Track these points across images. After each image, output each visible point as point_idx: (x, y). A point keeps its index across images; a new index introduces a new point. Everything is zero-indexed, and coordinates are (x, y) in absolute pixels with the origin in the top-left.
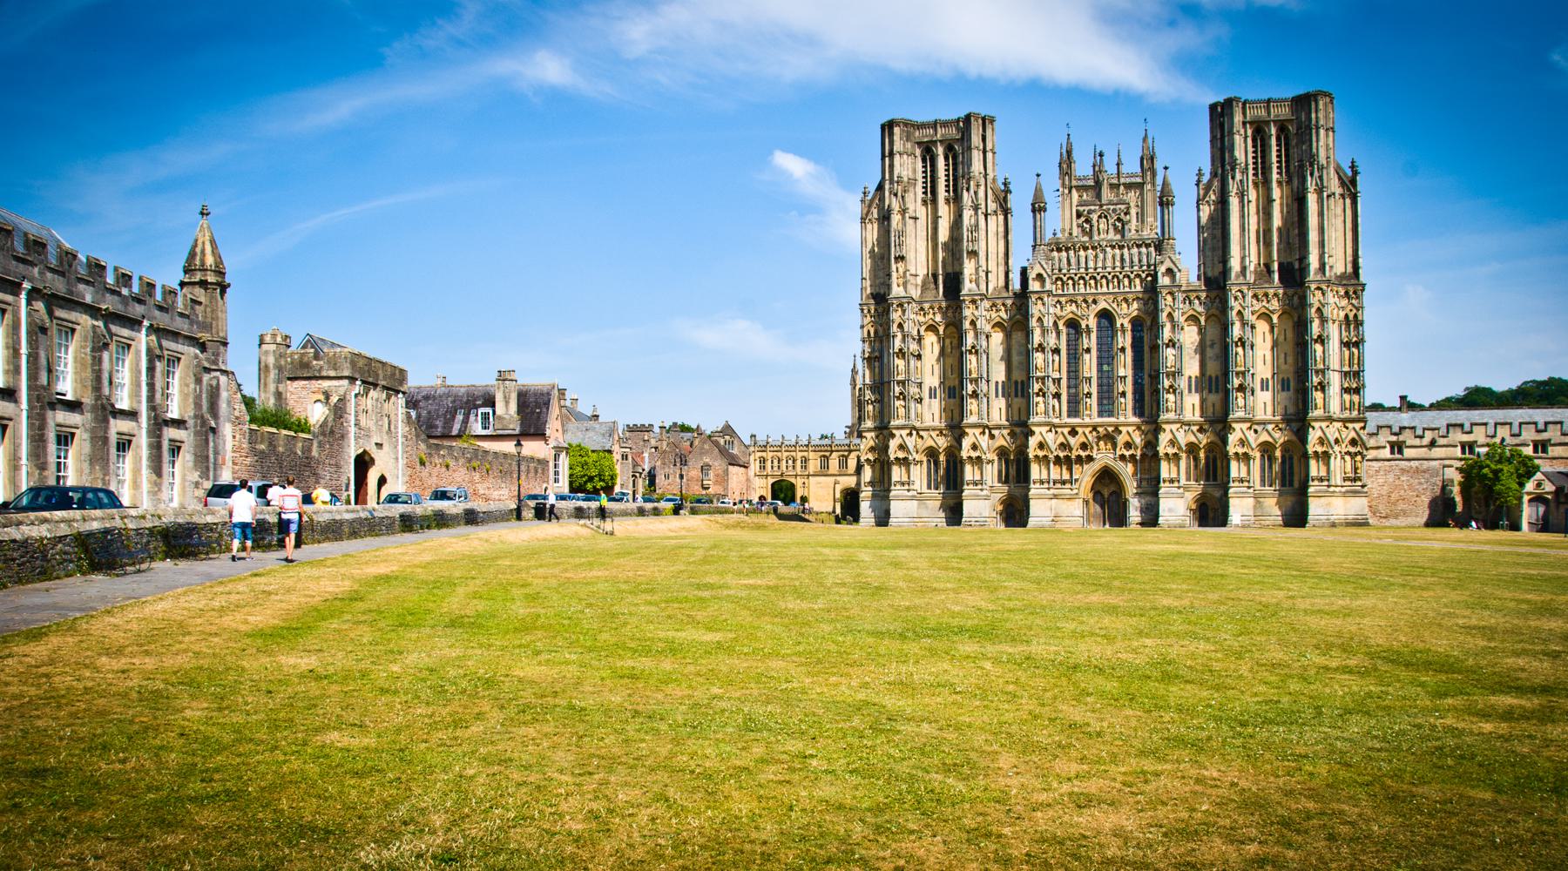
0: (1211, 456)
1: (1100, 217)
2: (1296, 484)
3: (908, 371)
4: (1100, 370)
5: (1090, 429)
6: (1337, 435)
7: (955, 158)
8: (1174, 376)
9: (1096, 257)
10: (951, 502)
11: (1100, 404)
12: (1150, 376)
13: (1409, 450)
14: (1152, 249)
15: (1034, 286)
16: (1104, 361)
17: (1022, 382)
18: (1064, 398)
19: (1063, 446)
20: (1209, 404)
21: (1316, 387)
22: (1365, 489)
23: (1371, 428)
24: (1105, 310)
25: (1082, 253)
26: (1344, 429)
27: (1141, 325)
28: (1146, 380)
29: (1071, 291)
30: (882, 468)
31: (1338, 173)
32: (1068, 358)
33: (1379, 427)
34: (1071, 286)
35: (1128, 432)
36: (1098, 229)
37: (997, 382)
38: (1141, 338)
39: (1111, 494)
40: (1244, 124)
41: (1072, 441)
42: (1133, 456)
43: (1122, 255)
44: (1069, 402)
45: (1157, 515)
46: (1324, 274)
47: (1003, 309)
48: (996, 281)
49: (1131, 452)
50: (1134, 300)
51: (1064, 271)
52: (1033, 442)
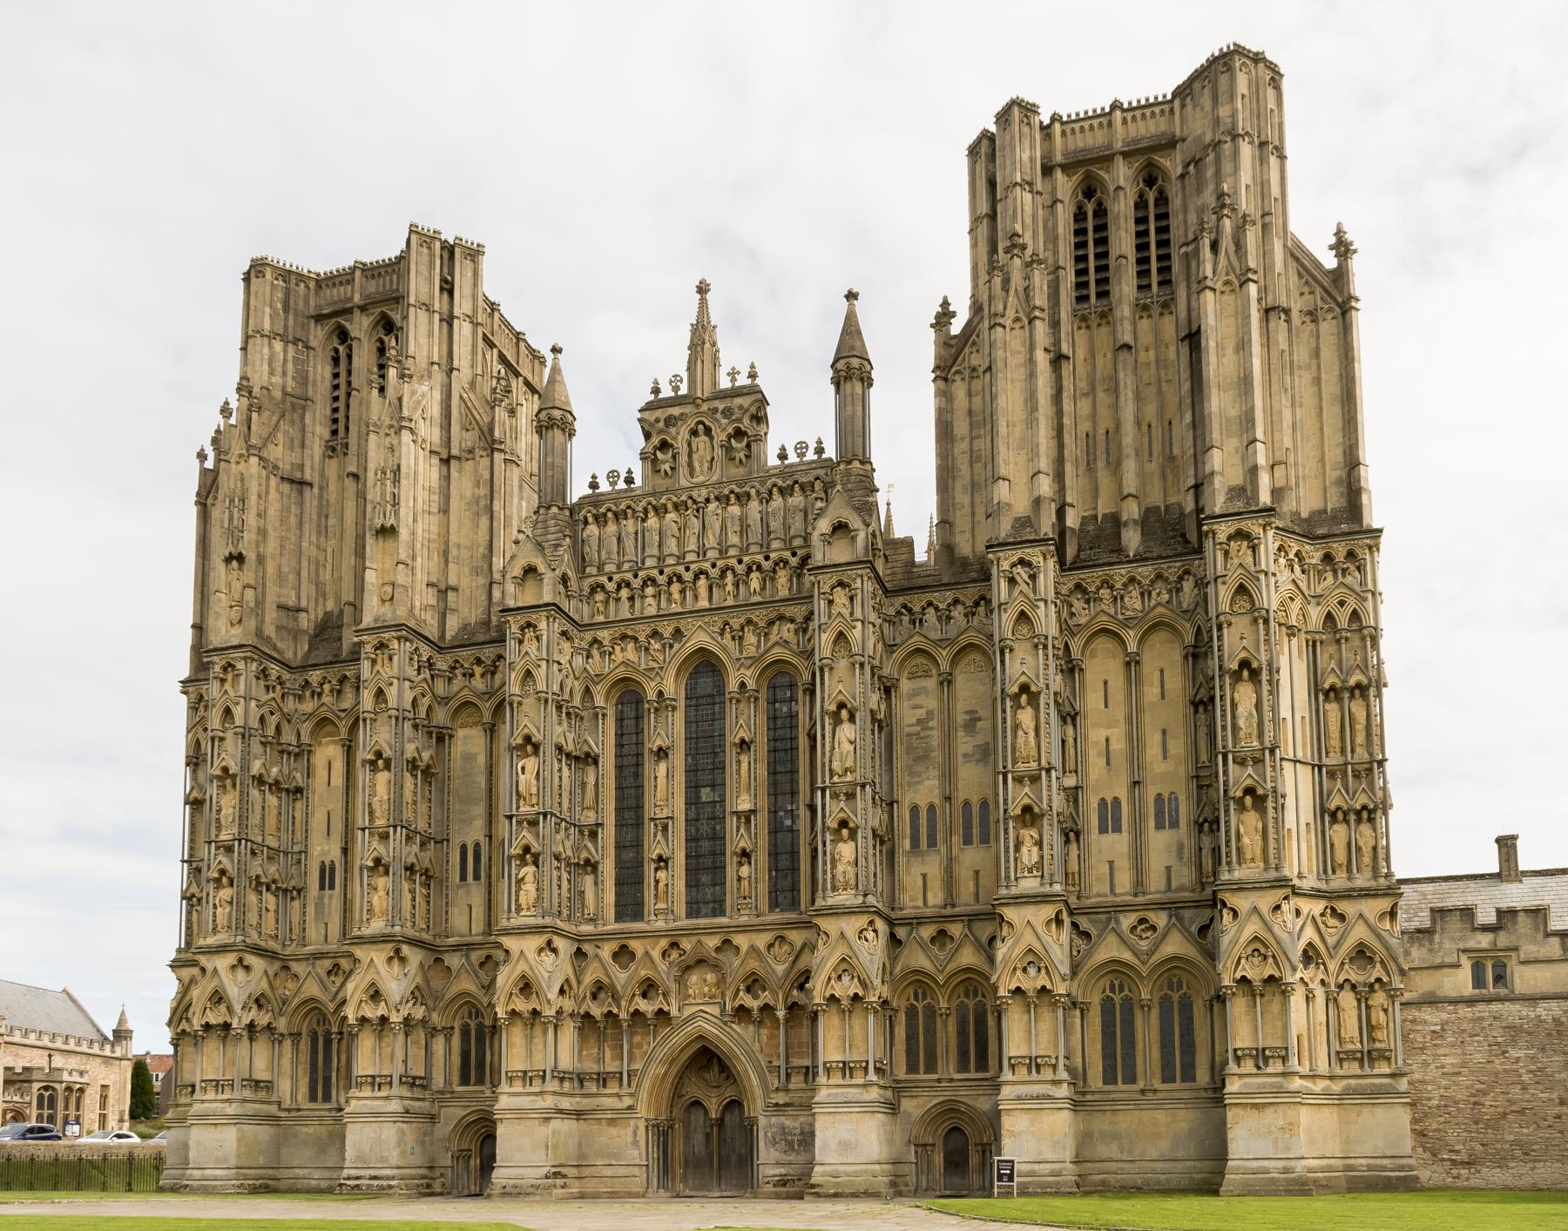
1: (694, 433)
3: (242, 819)
4: (692, 801)
6: (1310, 934)
9: (682, 529)
16: (705, 777)
22: (1403, 1085)
24: (702, 650)
25: (653, 521)
26: (1332, 922)
27: (792, 686)
29: (625, 613)
32: (619, 777)
36: (690, 465)
38: (793, 716)
43: (743, 519)
47: (478, 670)
50: (771, 623)
51: (610, 568)
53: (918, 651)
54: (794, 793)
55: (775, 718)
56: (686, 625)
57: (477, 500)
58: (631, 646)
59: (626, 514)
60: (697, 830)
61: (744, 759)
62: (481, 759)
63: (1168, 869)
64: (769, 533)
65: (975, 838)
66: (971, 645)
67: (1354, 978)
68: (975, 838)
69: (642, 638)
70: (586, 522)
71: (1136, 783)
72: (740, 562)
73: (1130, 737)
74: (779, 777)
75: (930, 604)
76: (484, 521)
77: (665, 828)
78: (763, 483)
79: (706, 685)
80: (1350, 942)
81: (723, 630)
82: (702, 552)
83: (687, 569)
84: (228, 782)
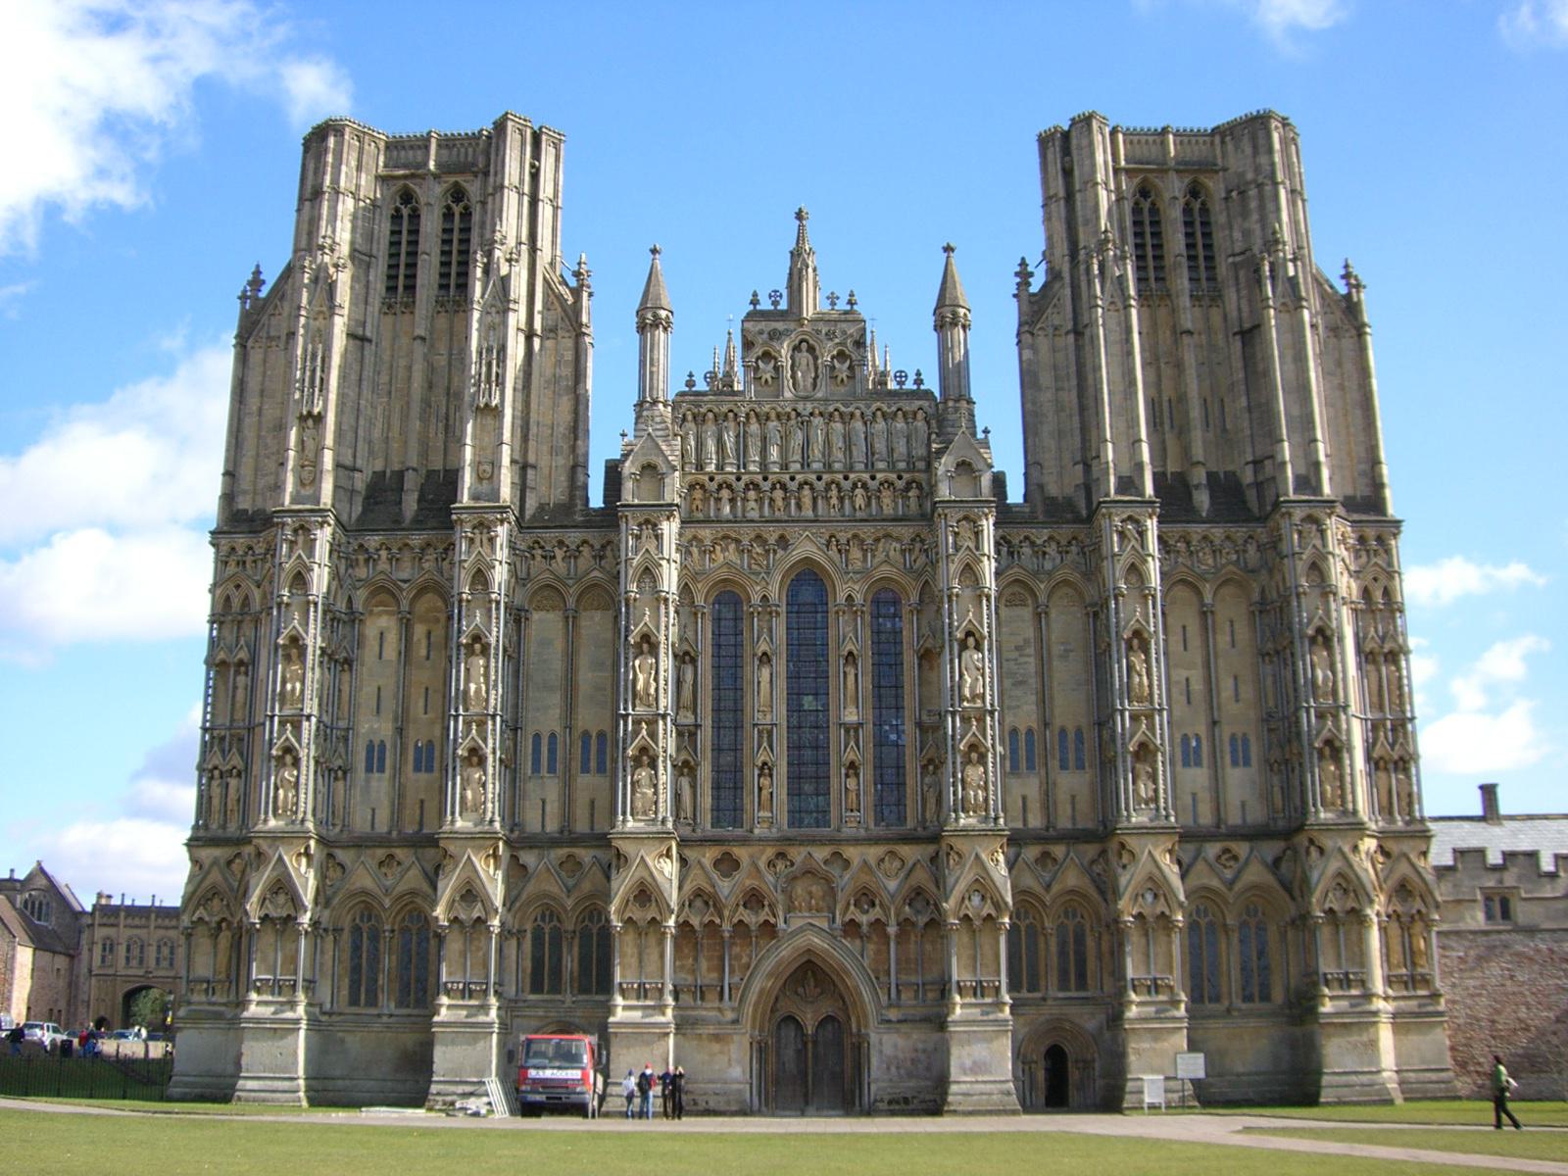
0: (1071, 924)
1: (796, 348)
2: (1278, 995)
4: (794, 707)
5: (770, 852)
7: (467, 214)
8: (981, 720)
9: (785, 438)
10: (409, 1040)
11: (794, 792)
12: (919, 725)
13: (1527, 906)
14: (920, 424)
15: (628, 496)
17: (601, 735)
18: (705, 772)
19: (701, 898)
20: (1062, 796)
21: (1320, 752)
23: (1440, 854)
24: (807, 560)
25: (754, 427)
26: (1381, 859)
27: (896, 602)
28: (910, 734)
30: (236, 945)
31: (1320, 285)
33: (1460, 853)
34: (727, 509)
35: (865, 862)
36: (793, 377)
37: (537, 737)
38: (897, 633)
39: (822, 1023)
40: (1116, 171)
41: (725, 887)
42: (878, 925)
44: (717, 787)
45: (942, 1082)
46: (1317, 489)
47: (559, 553)
48: (549, 490)
49: (876, 913)
50: (877, 540)
52: (622, 886)
53: (1017, 581)
54: (899, 708)
55: (879, 632)
56: (791, 531)
57: (556, 379)
58: (732, 547)
59: (726, 416)
60: (800, 738)
61: (851, 671)
62: (559, 645)
63: (1243, 805)
64: (873, 454)
65: (1072, 763)
66: (1066, 582)
67: (1399, 909)
68: (1072, 763)
69: (746, 542)
70: (684, 419)
71: (1215, 723)
72: (846, 478)
73: (1208, 680)
74: (883, 691)
75: (1027, 538)
76: (566, 403)
77: (770, 734)
78: (869, 407)
79: (807, 595)
80: (1396, 876)
81: (829, 542)
82: (805, 464)
83: (792, 479)
84: (294, 652)
